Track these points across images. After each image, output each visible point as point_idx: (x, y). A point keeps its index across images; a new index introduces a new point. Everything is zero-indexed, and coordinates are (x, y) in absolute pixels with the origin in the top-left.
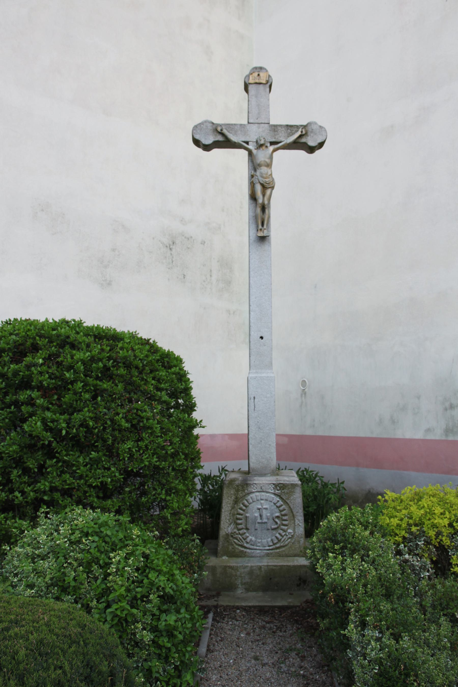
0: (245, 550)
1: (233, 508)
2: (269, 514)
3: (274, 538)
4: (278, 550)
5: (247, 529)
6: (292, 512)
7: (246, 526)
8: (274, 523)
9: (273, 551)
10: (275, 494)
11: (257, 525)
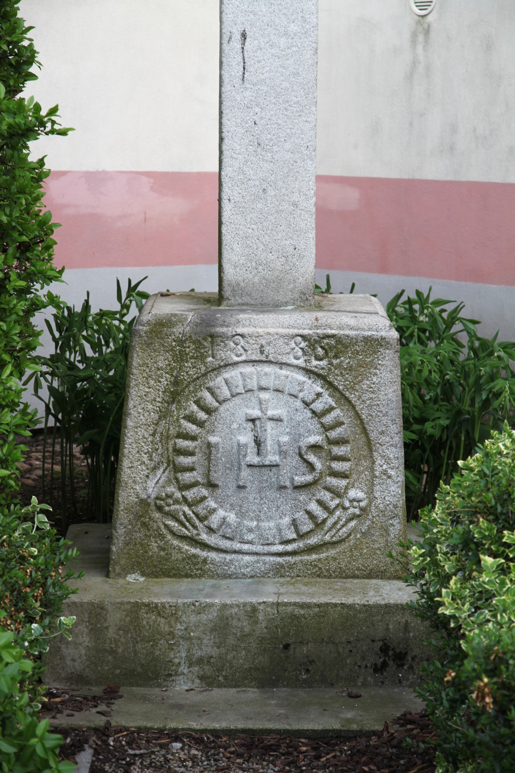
0: (204, 554)
1: (164, 415)
2: (285, 439)
3: (301, 515)
4: (314, 557)
5: (212, 486)
6: (365, 431)
7: (207, 475)
8: (303, 468)
9: (298, 558)
10: (308, 372)
11: (245, 473)
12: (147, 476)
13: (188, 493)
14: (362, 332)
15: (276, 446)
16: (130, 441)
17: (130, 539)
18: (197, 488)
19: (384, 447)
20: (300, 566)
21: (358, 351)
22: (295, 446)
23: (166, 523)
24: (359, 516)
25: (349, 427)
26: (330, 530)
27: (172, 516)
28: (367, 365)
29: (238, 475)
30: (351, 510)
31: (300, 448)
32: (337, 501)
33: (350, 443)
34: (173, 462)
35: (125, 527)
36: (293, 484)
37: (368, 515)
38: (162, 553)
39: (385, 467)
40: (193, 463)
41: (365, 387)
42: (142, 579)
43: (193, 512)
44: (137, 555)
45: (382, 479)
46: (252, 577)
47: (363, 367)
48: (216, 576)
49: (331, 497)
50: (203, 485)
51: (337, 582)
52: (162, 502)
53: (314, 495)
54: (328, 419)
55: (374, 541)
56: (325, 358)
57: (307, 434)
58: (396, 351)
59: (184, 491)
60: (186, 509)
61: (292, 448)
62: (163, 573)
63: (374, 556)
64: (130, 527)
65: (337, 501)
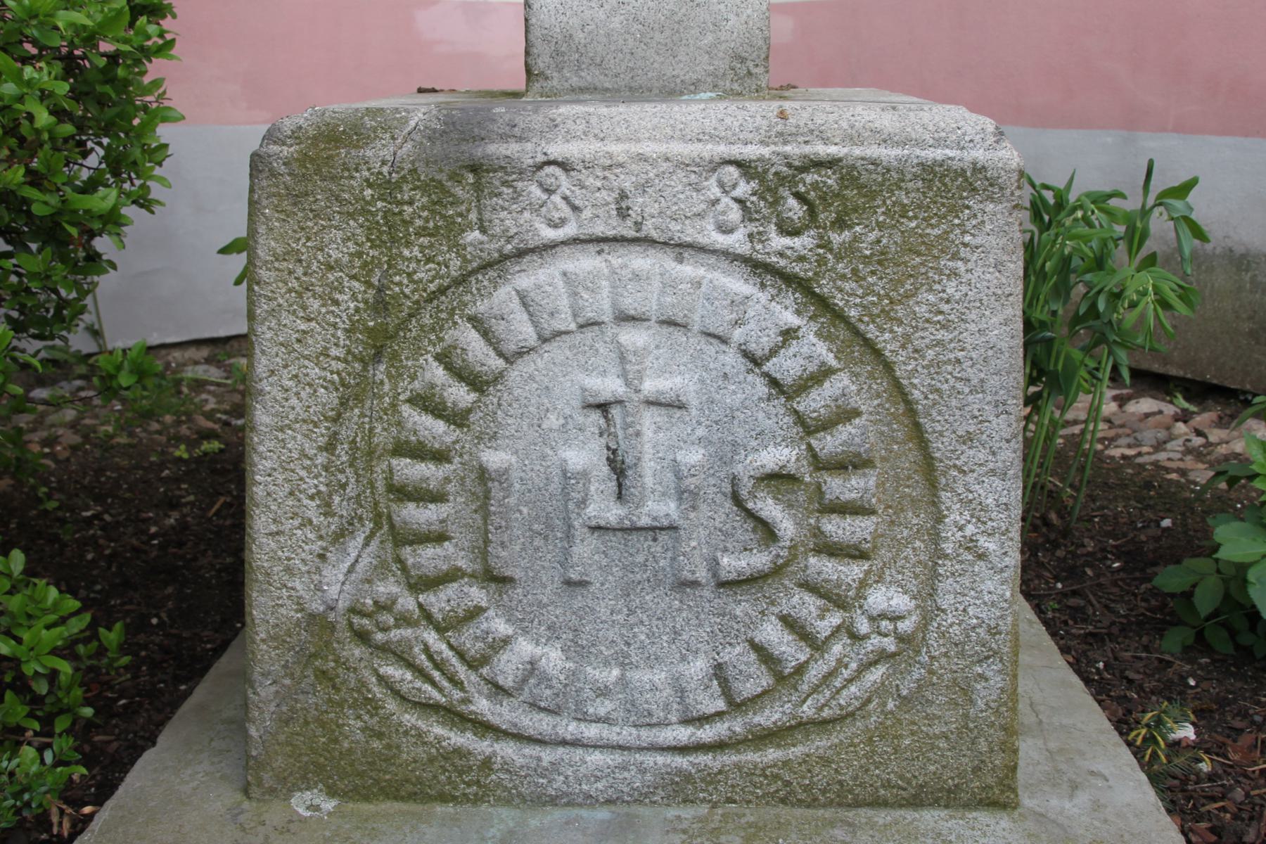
0: (483, 746)
1: (353, 393)
2: (693, 456)
3: (736, 654)
4: (772, 754)
5: (495, 579)
6: (918, 434)
7: (482, 550)
8: (744, 532)
9: (729, 758)
10: (758, 268)
11: (585, 549)
12: (322, 557)
13: (432, 599)
14: (918, 152)
15: (670, 475)
16: (268, 464)
17: (293, 710)
18: (455, 585)
19: (970, 478)
20: (735, 778)
21: (904, 206)
22: (722, 475)
23: (382, 671)
24: (893, 655)
25: (874, 423)
26: (815, 689)
27: (394, 653)
28: (930, 246)
29: (567, 553)
30: (875, 641)
31: (734, 481)
32: (835, 619)
33: (874, 467)
34: (389, 517)
35: (275, 682)
36: (715, 575)
37: (918, 652)
38: (376, 744)
39: (970, 530)
40: (442, 521)
41: (921, 310)
42: (329, 805)
43: (451, 647)
44: (312, 749)
45: (961, 562)
46: (609, 802)
47: (919, 254)
48: (517, 800)
49: (819, 608)
50: (473, 576)
51: (832, 824)
52: (365, 621)
53: (773, 603)
54: (815, 402)
55: (931, 718)
56: (808, 227)
57: (754, 443)
58: (1015, 207)
59: (422, 592)
60: (431, 637)
61: (712, 481)
62: (382, 789)
63: (931, 755)
64: (287, 682)
65: (835, 619)
